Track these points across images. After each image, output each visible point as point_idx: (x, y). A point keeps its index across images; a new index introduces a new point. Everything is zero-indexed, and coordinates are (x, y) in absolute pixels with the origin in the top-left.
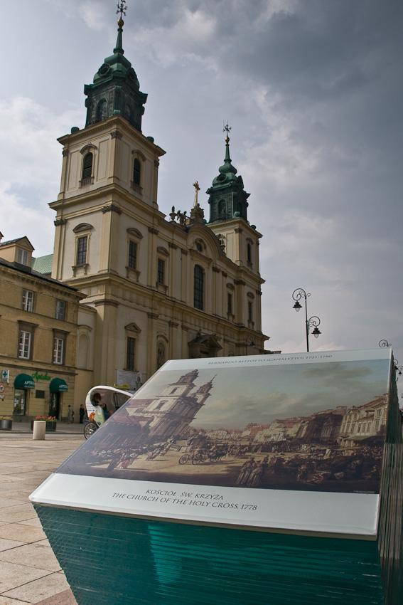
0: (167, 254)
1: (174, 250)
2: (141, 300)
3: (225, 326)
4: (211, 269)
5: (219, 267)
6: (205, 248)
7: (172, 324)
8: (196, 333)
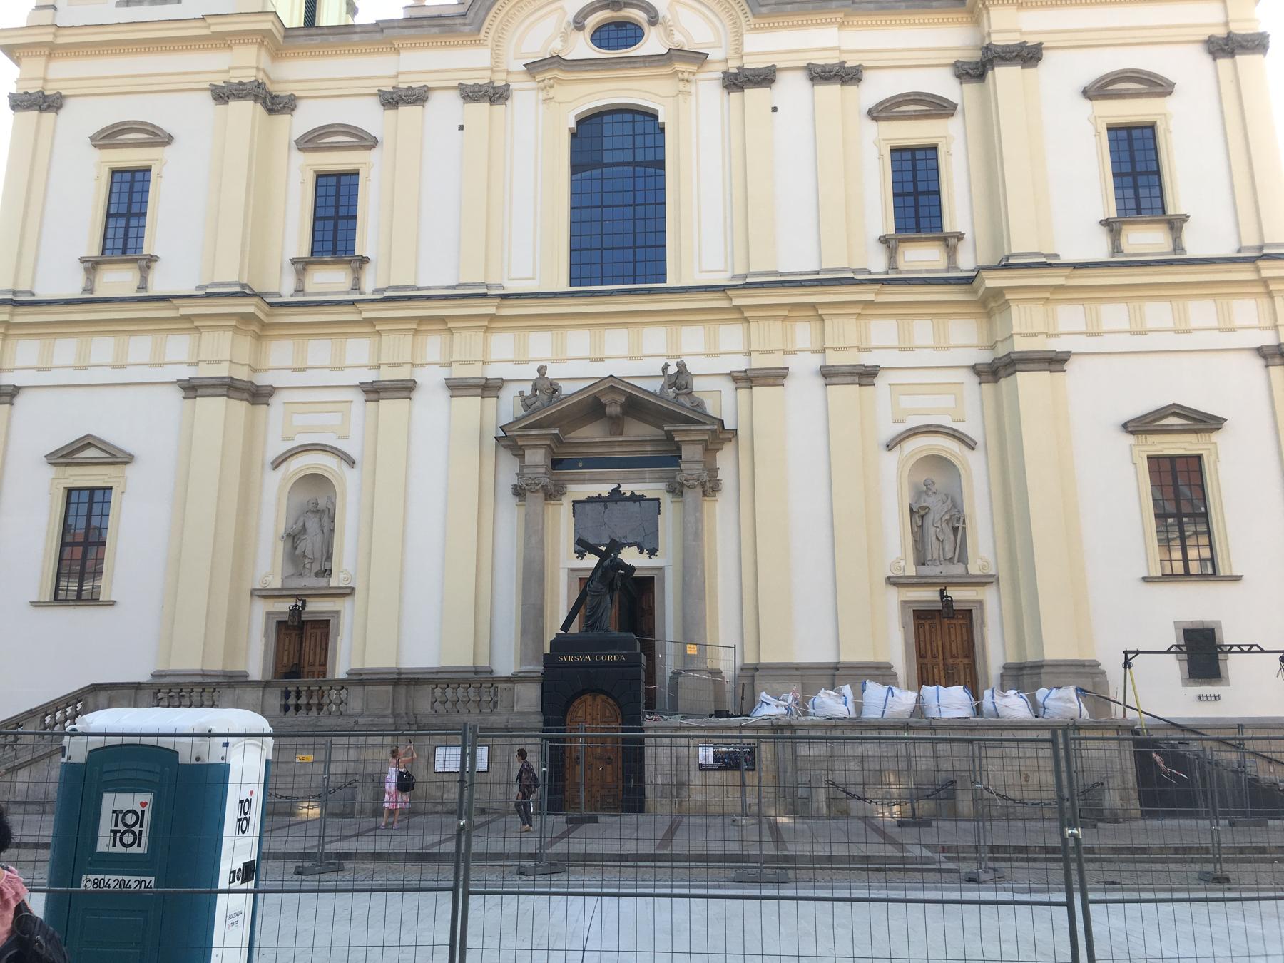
0: (366, 141)
1: (404, 110)
2: (140, 347)
3: (813, 306)
4: (708, 87)
5: (751, 63)
6: (653, 21)
7: (375, 391)
8: (528, 390)
